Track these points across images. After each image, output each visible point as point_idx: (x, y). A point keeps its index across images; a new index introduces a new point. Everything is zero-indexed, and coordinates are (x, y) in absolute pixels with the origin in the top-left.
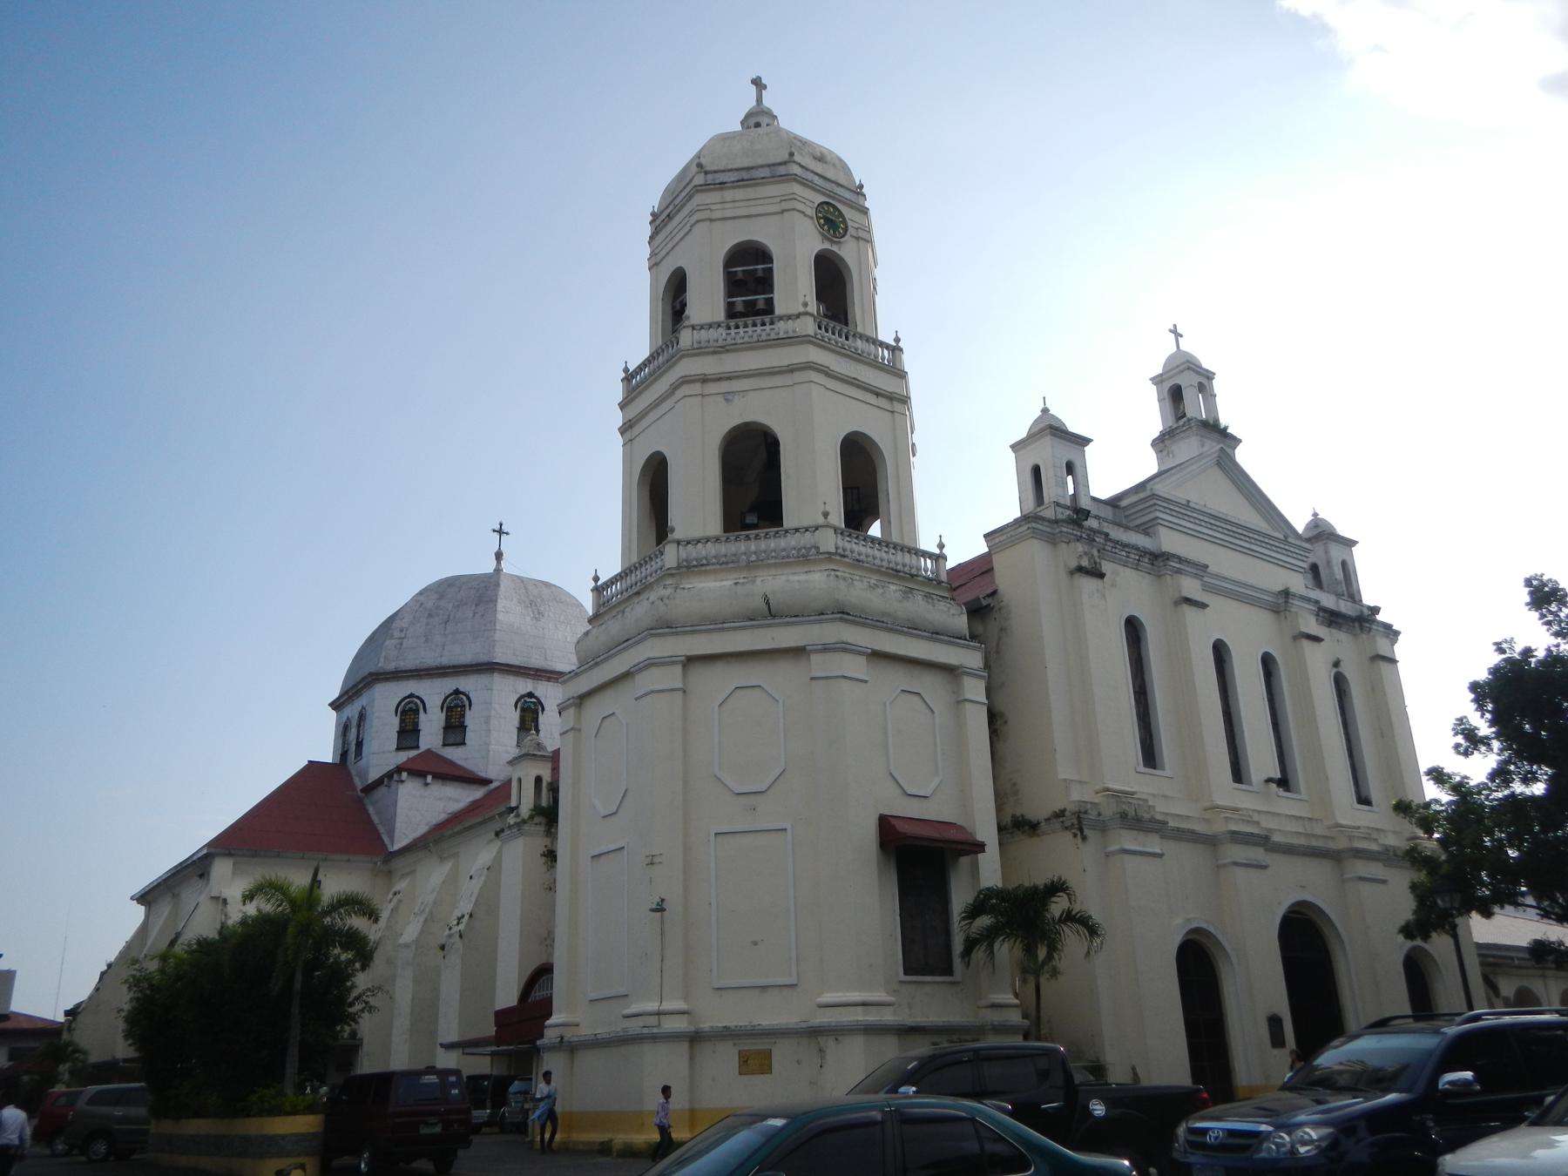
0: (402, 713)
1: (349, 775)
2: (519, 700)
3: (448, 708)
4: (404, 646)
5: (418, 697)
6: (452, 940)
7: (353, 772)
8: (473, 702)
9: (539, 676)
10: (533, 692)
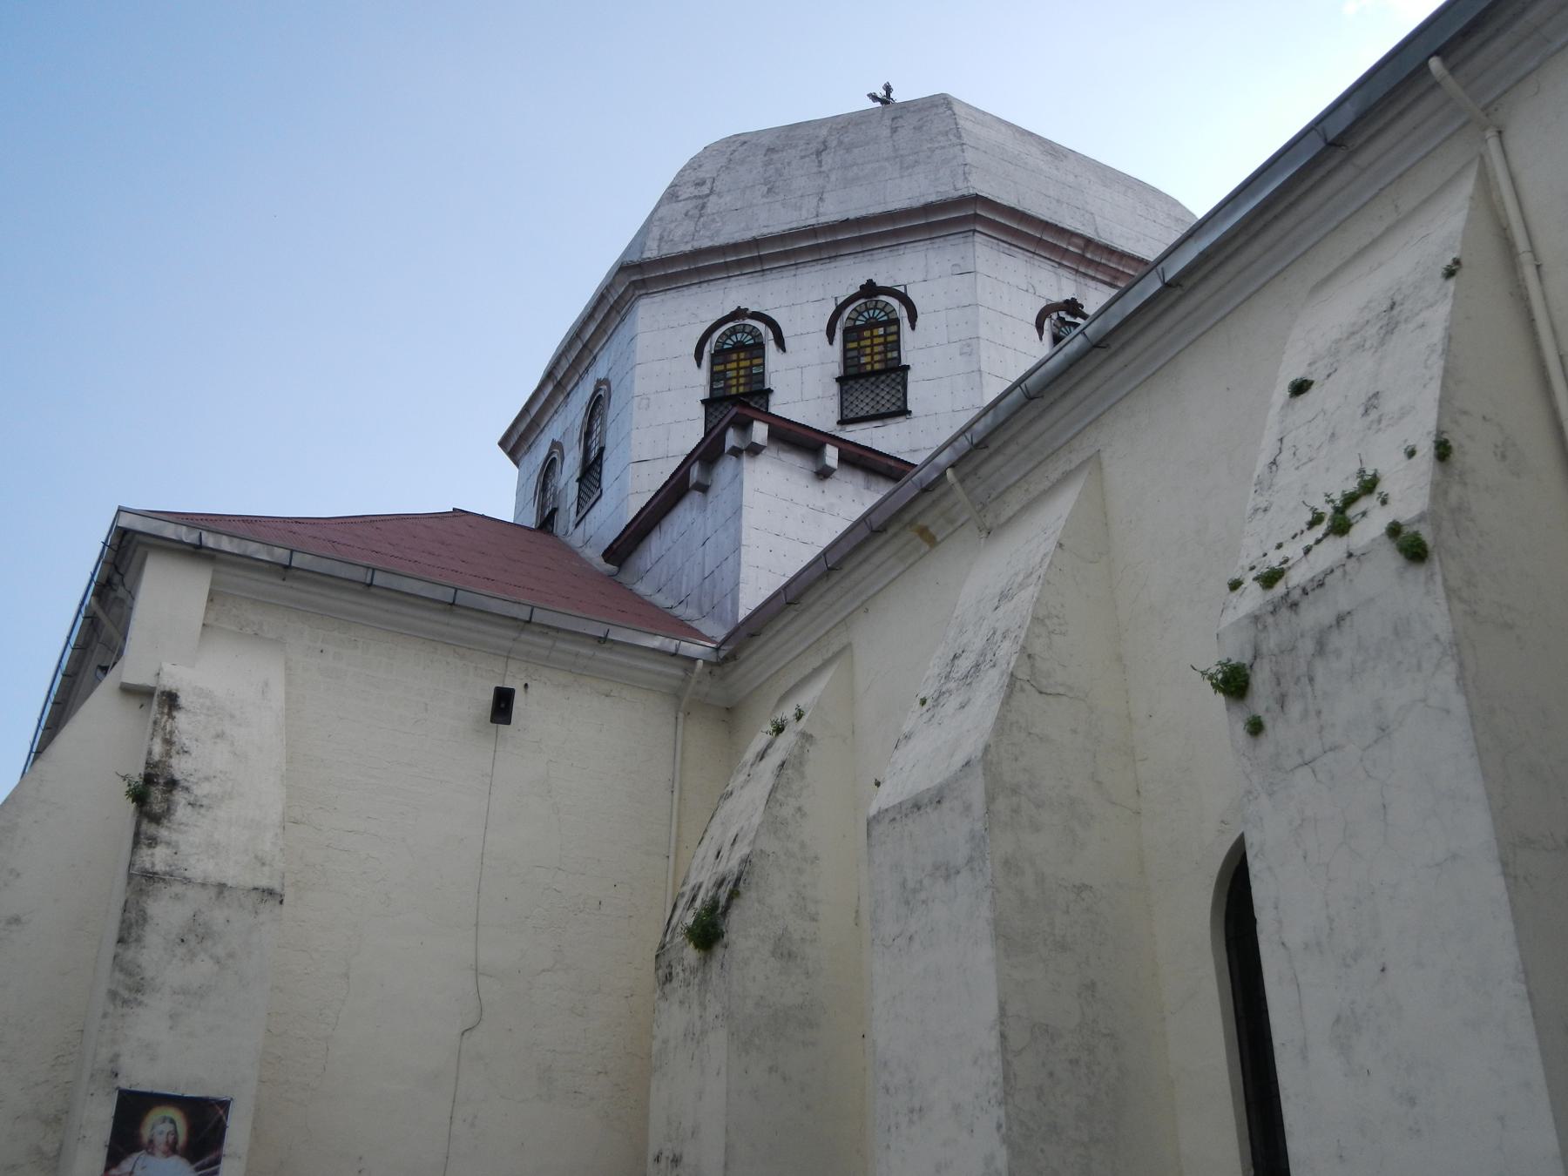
0: (713, 357)
3: (846, 331)
4: (709, 210)
9: (1090, 263)
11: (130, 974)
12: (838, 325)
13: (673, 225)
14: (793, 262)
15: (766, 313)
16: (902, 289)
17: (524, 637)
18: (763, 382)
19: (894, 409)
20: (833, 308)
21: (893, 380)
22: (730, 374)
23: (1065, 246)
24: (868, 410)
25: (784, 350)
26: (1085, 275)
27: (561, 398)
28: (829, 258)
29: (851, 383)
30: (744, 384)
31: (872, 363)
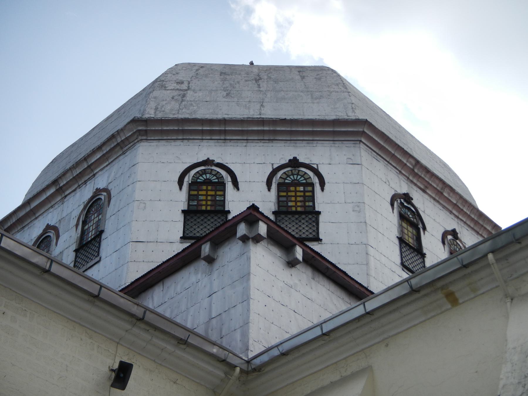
3: (279, 185)
8: (326, 181)
12: (274, 180)
13: (165, 102)
14: (245, 138)
15: (226, 165)
16: (315, 166)
17: (136, 330)
18: (224, 206)
19: (311, 236)
20: (271, 170)
21: (310, 219)
22: (201, 198)
23: (405, 161)
25: (238, 189)
26: (412, 182)
27: (59, 198)
28: (269, 140)
30: (211, 205)
31: (296, 206)
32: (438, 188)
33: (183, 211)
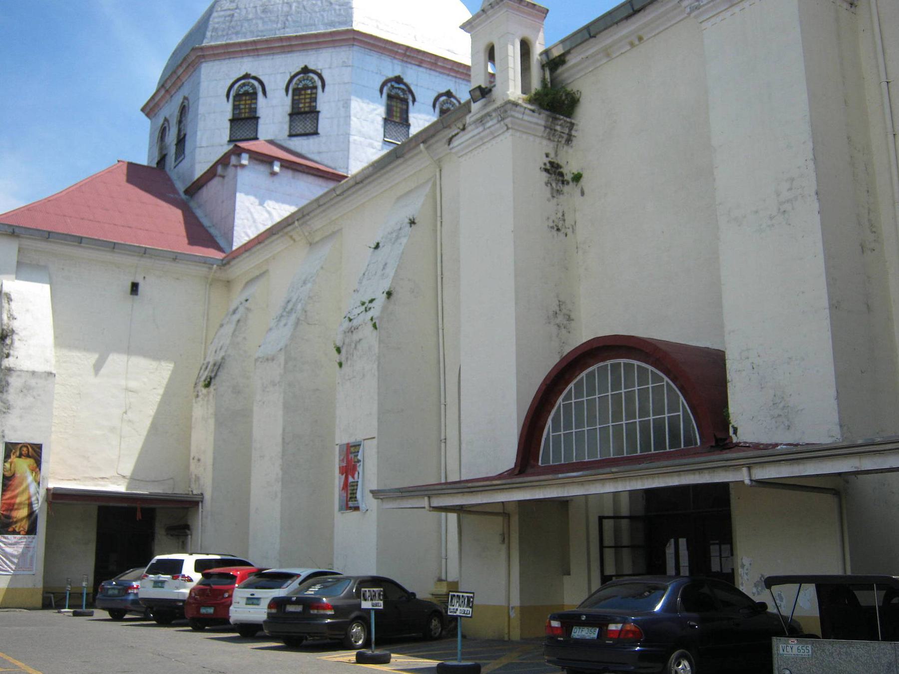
0: (235, 97)
1: (169, 179)
2: (384, 84)
3: (294, 90)
4: (235, 19)
5: (255, 78)
6: (356, 337)
7: (174, 177)
8: (326, 83)
9: (409, 56)
10: (402, 77)
11: (5, 403)
16: (319, 71)
21: (313, 117)
23: (396, 50)
24: (301, 131)
26: (406, 62)
29: (294, 116)
30: (248, 113)
31: (304, 107)
32: (432, 61)
33: (230, 120)
